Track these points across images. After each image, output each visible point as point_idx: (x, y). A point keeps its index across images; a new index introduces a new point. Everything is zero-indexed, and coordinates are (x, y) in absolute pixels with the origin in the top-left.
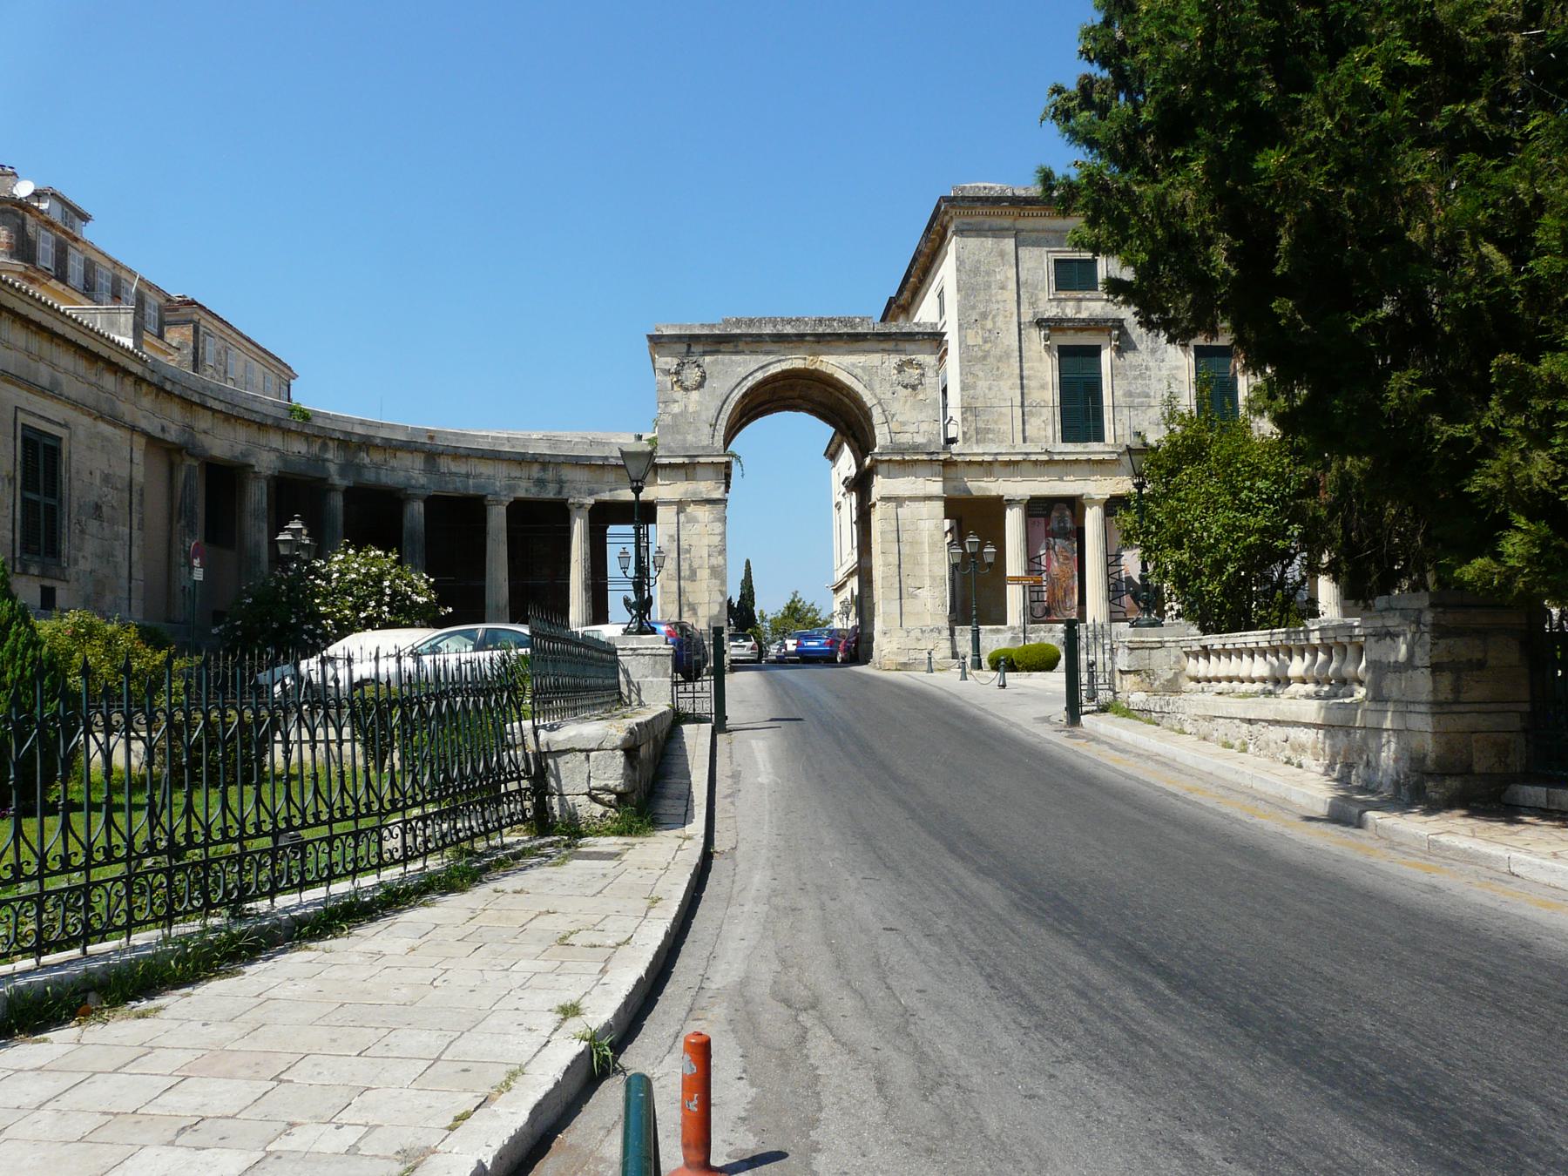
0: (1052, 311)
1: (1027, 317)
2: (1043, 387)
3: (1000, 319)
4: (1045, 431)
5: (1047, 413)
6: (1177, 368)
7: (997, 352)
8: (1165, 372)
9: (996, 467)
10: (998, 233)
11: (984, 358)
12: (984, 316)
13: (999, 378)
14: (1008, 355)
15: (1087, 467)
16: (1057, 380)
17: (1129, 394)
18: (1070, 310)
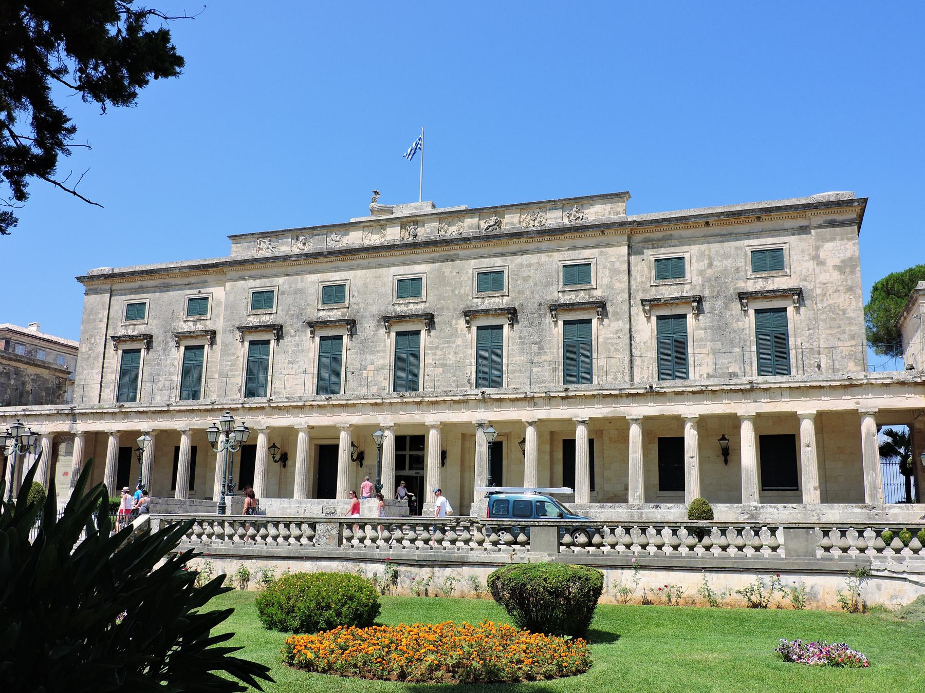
0: (121, 332)
1: (111, 333)
2: (112, 372)
3: (98, 337)
4: (646, 372)
5: (112, 386)
6: (175, 359)
7: (94, 355)
8: (169, 362)
9: (8, 418)
10: (102, 292)
11: (88, 358)
12: (91, 336)
13: (93, 368)
14: (98, 356)
15: (44, 417)
16: (119, 368)
17: (151, 374)
18: (130, 332)
